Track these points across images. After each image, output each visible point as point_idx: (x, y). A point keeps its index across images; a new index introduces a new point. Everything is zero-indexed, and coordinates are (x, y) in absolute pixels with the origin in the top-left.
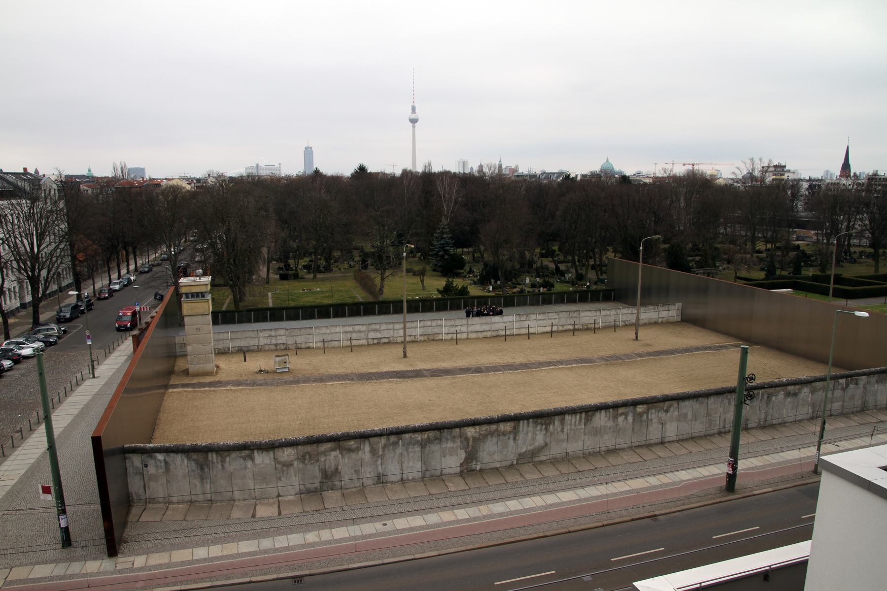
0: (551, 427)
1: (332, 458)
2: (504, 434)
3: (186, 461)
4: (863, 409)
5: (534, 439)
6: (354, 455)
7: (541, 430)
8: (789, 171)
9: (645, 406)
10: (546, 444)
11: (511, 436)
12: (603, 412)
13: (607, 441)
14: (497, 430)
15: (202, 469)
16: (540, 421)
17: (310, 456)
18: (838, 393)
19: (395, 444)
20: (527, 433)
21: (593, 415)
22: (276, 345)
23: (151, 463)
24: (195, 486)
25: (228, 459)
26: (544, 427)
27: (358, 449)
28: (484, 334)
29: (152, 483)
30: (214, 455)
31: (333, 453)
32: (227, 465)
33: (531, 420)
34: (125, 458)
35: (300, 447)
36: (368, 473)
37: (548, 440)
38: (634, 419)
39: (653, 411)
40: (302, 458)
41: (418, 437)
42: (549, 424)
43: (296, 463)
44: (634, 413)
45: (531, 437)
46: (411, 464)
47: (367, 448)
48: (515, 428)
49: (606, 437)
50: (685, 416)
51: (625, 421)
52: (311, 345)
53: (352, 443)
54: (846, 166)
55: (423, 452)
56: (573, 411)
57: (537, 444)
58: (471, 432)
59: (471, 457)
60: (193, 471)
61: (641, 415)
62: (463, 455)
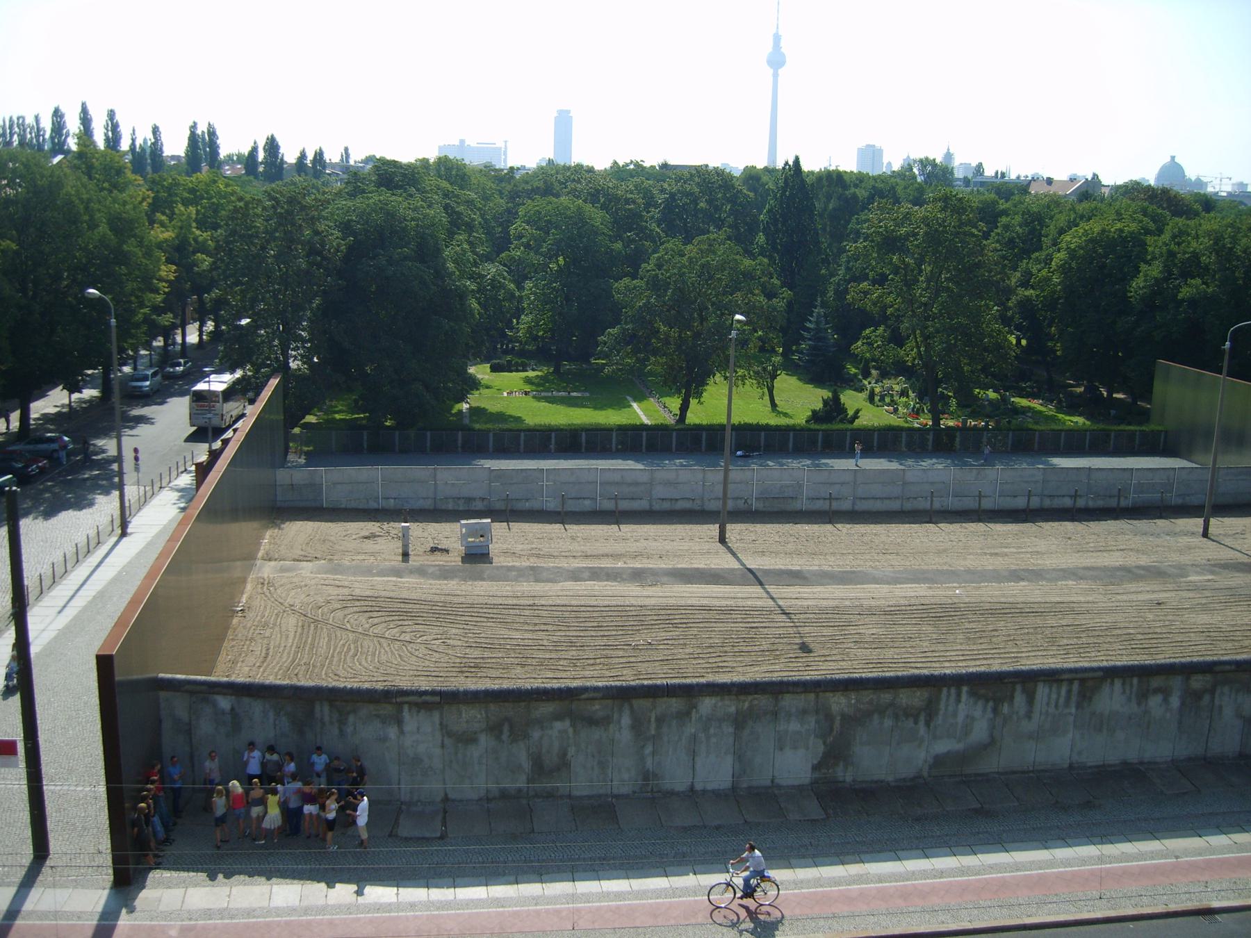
0: (1005, 709)
3: (271, 715)
6: (597, 734)
9: (1208, 677)
11: (922, 718)
14: (892, 704)
16: (982, 691)
17: (511, 727)
19: (684, 716)
25: (351, 718)
26: (991, 704)
27: (605, 722)
30: (326, 709)
31: (558, 725)
32: (350, 729)
33: (965, 689)
35: (492, 707)
38: (1183, 704)
39: (1226, 689)
40: (494, 729)
43: (483, 738)
47: (626, 720)
56: (1051, 676)
58: (838, 703)
61: (1197, 695)
62: (818, 748)
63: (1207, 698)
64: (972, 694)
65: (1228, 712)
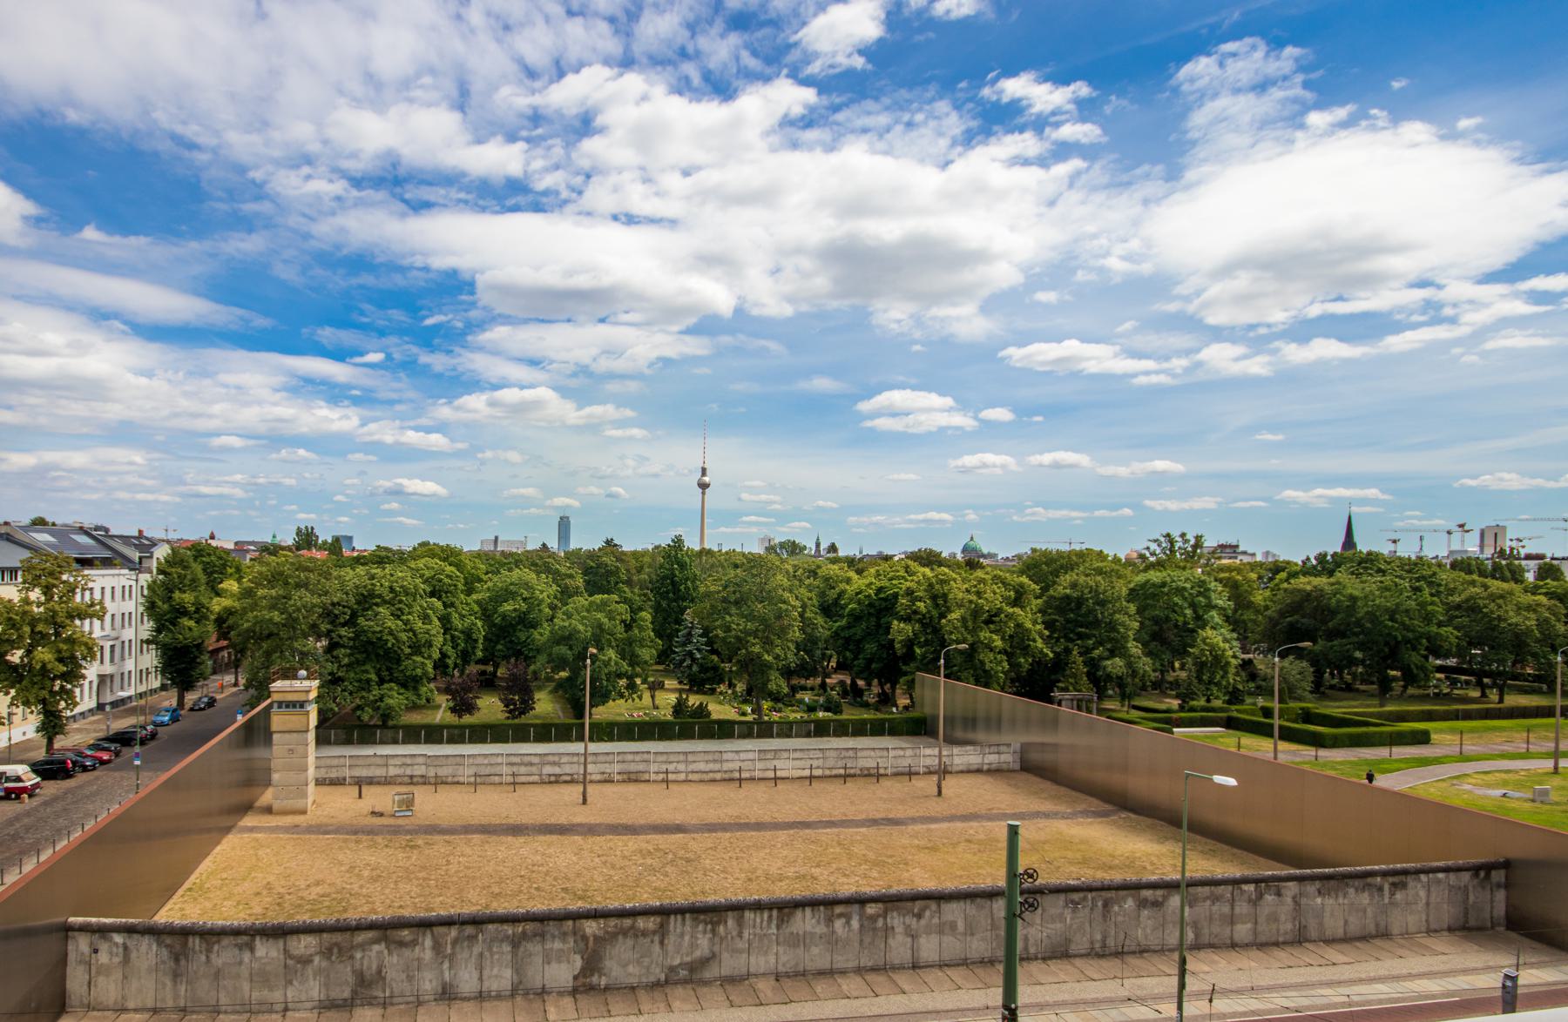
0: (722, 928)
1: (373, 954)
2: (644, 933)
3: (154, 947)
4: (1299, 939)
5: (693, 946)
6: (407, 952)
7: (705, 932)
8: (1244, 553)
9: (880, 905)
10: (714, 956)
11: (657, 938)
12: (808, 910)
13: (817, 957)
14: (633, 927)
15: (177, 960)
17: (340, 950)
18: (1242, 908)
19: (472, 938)
20: (682, 935)
21: (790, 915)
22: (411, 777)
23: (104, 947)
24: (164, 985)
25: (216, 947)
27: (414, 943)
28: (711, 776)
29: (101, 979)
30: (197, 941)
31: (376, 948)
32: (213, 956)
34: (67, 937)
35: (325, 935)
36: (428, 983)
37: (716, 948)
40: (327, 953)
41: (509, 929)
42: (719, 923)
43: (317, 959)
44: (862, 915)
45: (689, 941)
46: (495, 971)
47: (428, 942)
48: (662, 926)
49: (815, 950)
50: (953, 926)
51: (847, 927)
52: (461, 779)
53: (405, 934)
54: (1349, 542)
55: (514, 954)
56: (758, 906)
57: (698, 954)
58: (591, 927)
59: (592, 964)
60: (164, 962)
61: (873, 918)
63: (880, 923)
64: (695, 919)
65: (899, 929)
